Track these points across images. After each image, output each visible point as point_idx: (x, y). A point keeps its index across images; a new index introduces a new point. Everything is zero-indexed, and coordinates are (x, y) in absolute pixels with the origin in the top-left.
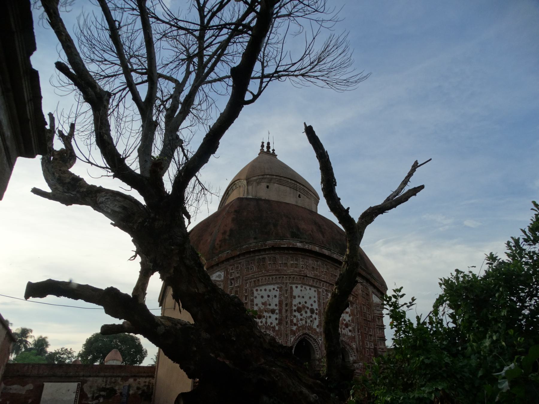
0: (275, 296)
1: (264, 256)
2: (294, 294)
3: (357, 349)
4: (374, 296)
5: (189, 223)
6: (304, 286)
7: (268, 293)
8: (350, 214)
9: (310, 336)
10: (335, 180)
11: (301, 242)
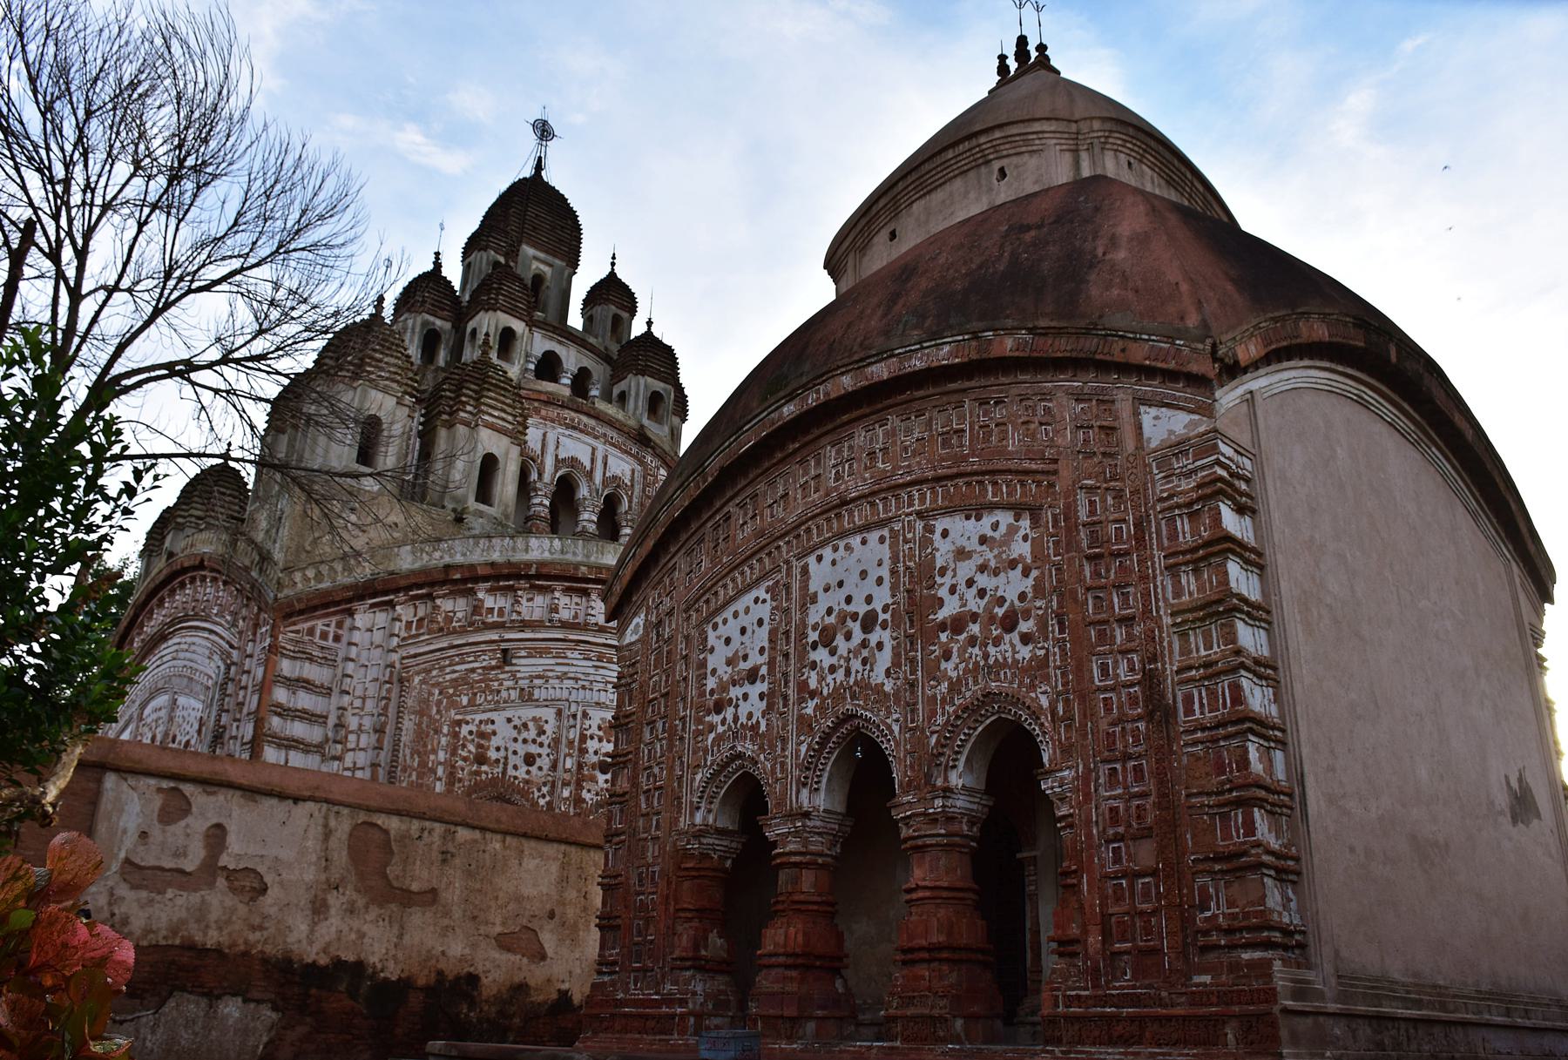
1: (726, 510)
6: (842, 544)
11: (790, 398)
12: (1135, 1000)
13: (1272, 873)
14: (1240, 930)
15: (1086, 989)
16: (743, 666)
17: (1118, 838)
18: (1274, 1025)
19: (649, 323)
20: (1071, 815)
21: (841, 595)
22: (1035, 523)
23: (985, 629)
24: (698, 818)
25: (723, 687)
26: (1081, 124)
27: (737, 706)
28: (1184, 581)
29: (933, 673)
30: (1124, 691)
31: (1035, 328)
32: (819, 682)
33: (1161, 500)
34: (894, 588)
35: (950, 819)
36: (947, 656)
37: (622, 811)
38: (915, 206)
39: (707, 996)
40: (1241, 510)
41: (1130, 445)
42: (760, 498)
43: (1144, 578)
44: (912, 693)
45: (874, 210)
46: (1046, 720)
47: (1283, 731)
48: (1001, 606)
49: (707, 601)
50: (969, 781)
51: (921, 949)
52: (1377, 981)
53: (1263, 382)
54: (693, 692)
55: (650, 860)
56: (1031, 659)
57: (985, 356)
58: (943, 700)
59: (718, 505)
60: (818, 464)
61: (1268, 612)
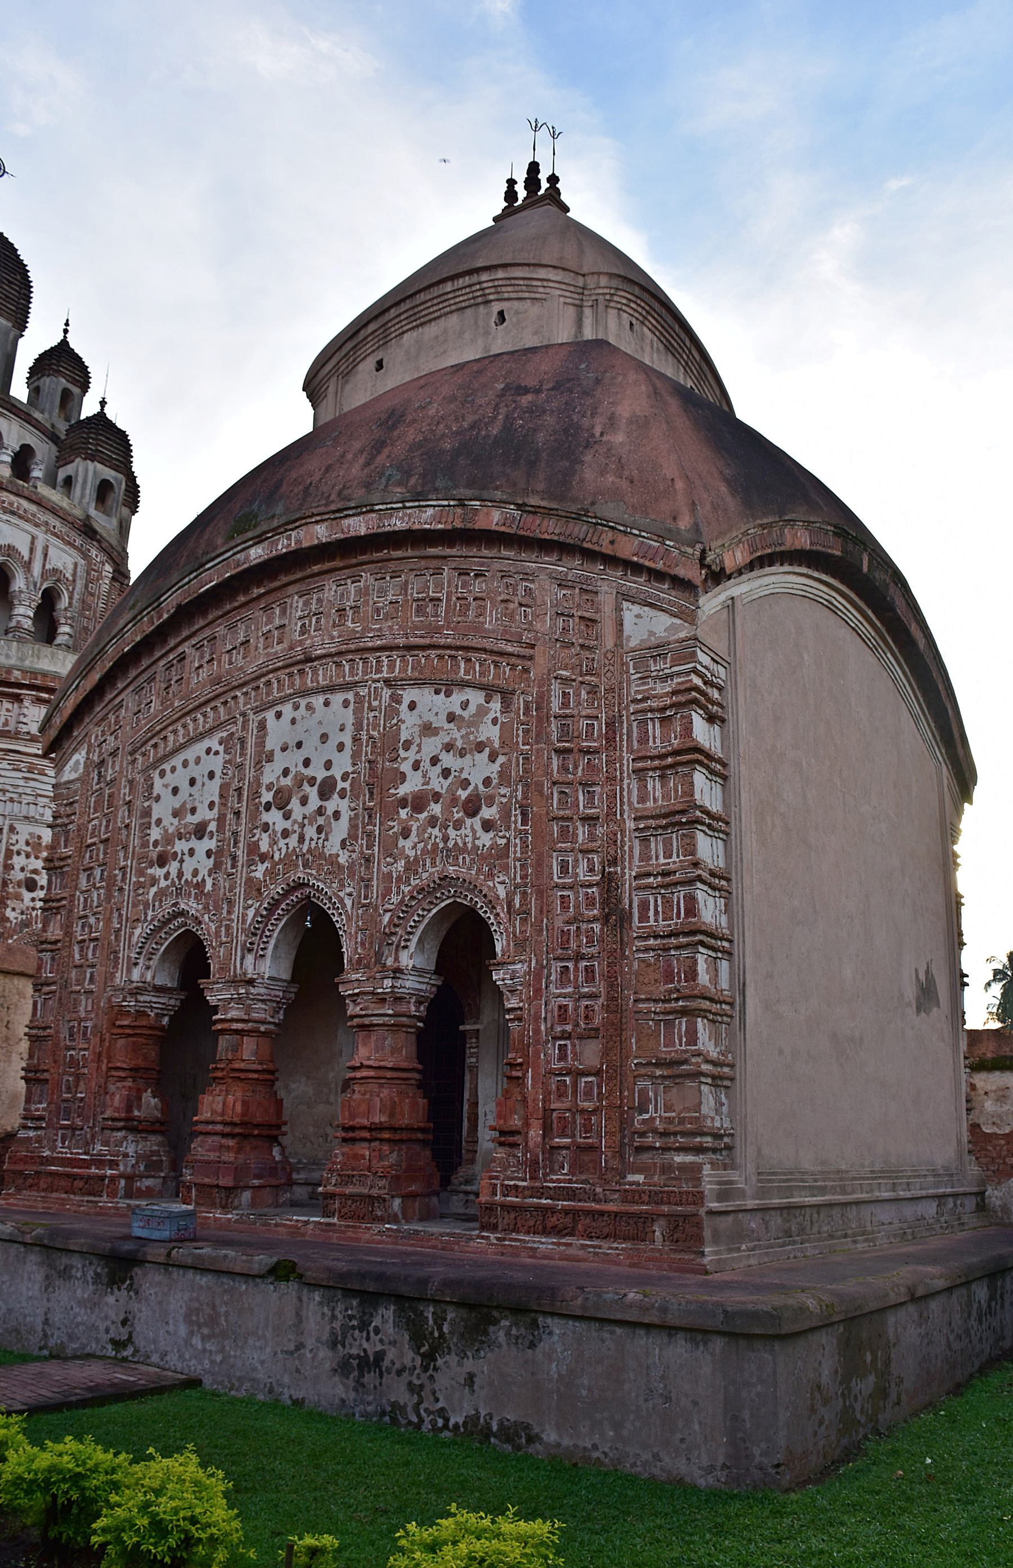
1: (180, 649)
3: (510, 904)
6: (303, 702)
11: (259, 540)
12: (571, 1194)
13: (709, 1080)
14: (675, 1134)
15: (525, 1180)
16: (190, 819)
17: (566, 1036)
18: (699, 1225)
19: (103, 403)
20: (520, 1009)
21: (300, 756)
22: (506, 707)
23: (447, 809)
24: (136, 974)
25: (168, 840)
26: (589, 279)
27: (182, 861)
28: (650, 787)
29: (390, 851)
30: (582, 891)
31: (525, 505)
32: (271, 846)
33: (635, 701)
34: (355, 756)
35: (399, 1000)
36: (406, 834)
37: (53, 959)
38: (405, 335)
39: (139, 1157)
40: (711, 719)
41: (609, 643)
42: (218, 642)
43: (611, 779)
44: (367, 868)
45: (363, 334)
46: (502, 911)
47: (731, 941)
48: (464, 789)
49: (155, 746)
50: (420, 962)
51: (363, 1128)
52: (791, 1173)
53: (744, 588)
54: (135, 841)
55: (83, 1015)
56: (491, 848)
57: (469, 526)
58: (399, 879)
59: (172, 643)
60: (283, 612)
61: (727, 823)
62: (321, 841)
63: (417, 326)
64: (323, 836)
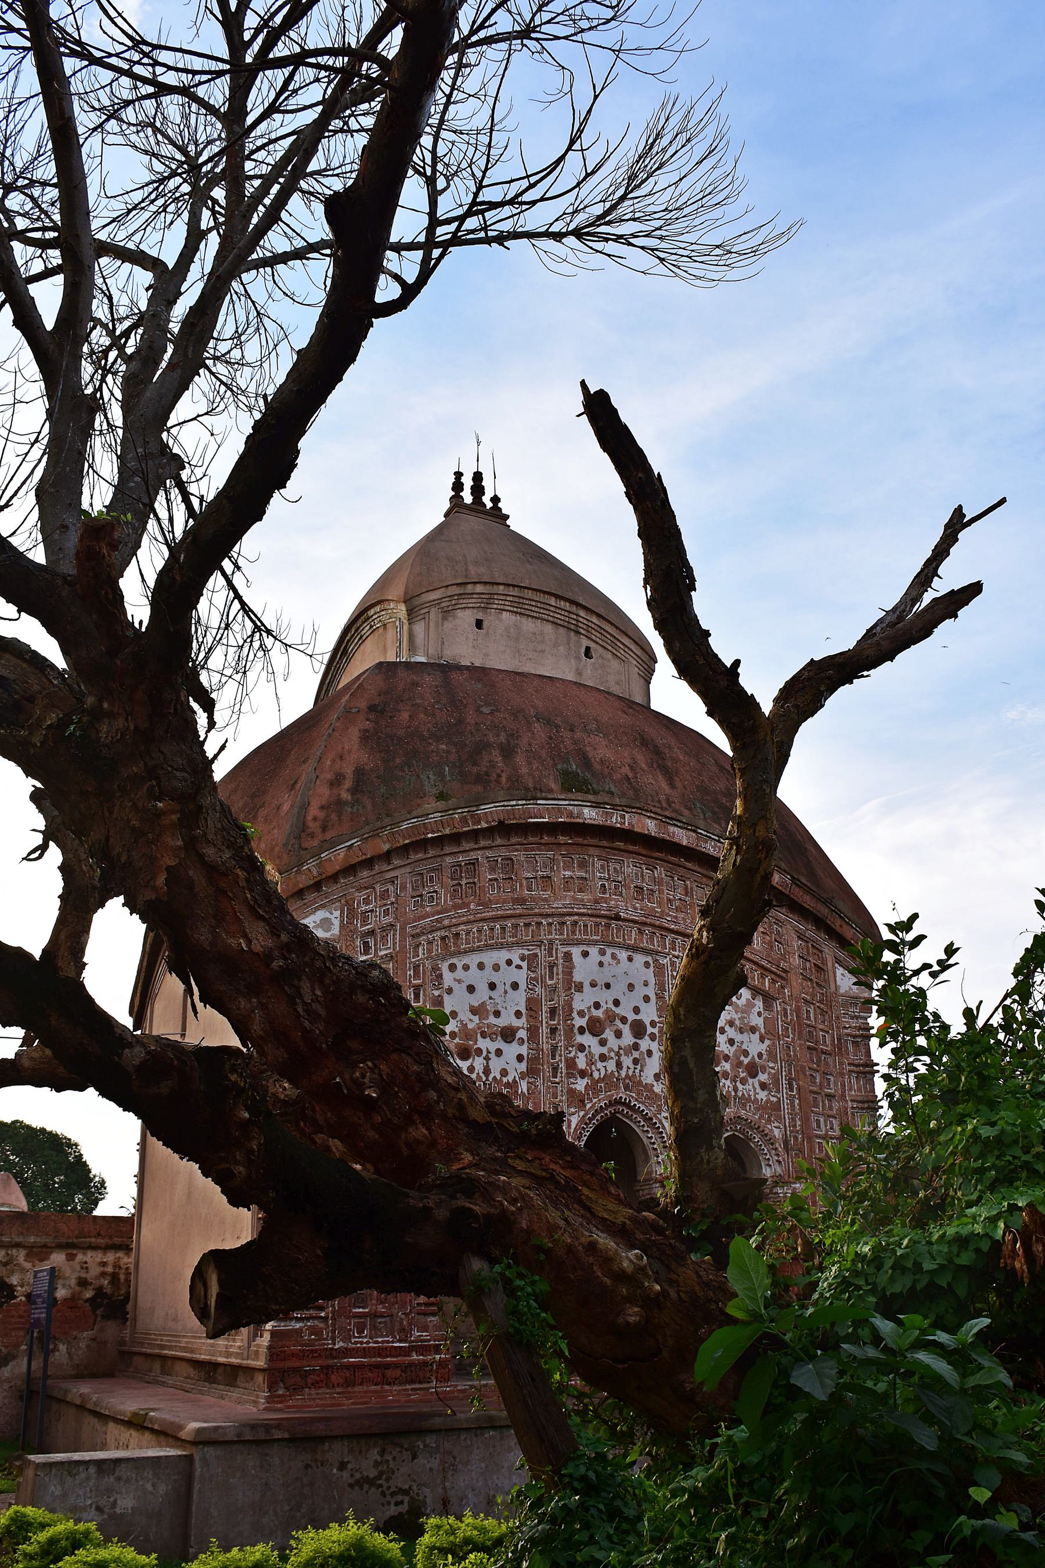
0: (515, 986)
1: (473, 855)
2: (577, 977)
3: (786, 1142)
4: (840, 971)
5: (212, 724)
6: (609, 951)
7: (489, 974)
8: (743, 681)
9: (633, 1108)
10: (690, 570)
11: (596, 805)
22: (768, 1007)
48: (746, 1057)
62: (637, 1071)
63: (520, 614)
64: (639, 1067)
